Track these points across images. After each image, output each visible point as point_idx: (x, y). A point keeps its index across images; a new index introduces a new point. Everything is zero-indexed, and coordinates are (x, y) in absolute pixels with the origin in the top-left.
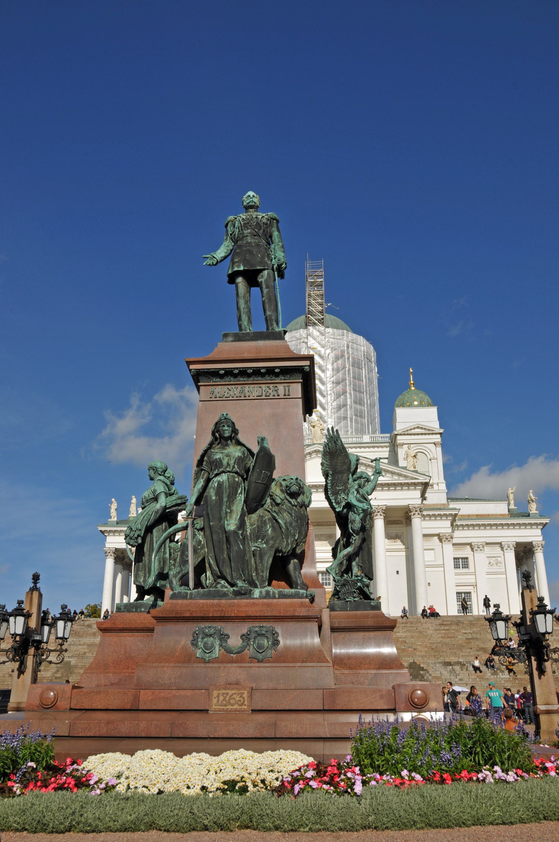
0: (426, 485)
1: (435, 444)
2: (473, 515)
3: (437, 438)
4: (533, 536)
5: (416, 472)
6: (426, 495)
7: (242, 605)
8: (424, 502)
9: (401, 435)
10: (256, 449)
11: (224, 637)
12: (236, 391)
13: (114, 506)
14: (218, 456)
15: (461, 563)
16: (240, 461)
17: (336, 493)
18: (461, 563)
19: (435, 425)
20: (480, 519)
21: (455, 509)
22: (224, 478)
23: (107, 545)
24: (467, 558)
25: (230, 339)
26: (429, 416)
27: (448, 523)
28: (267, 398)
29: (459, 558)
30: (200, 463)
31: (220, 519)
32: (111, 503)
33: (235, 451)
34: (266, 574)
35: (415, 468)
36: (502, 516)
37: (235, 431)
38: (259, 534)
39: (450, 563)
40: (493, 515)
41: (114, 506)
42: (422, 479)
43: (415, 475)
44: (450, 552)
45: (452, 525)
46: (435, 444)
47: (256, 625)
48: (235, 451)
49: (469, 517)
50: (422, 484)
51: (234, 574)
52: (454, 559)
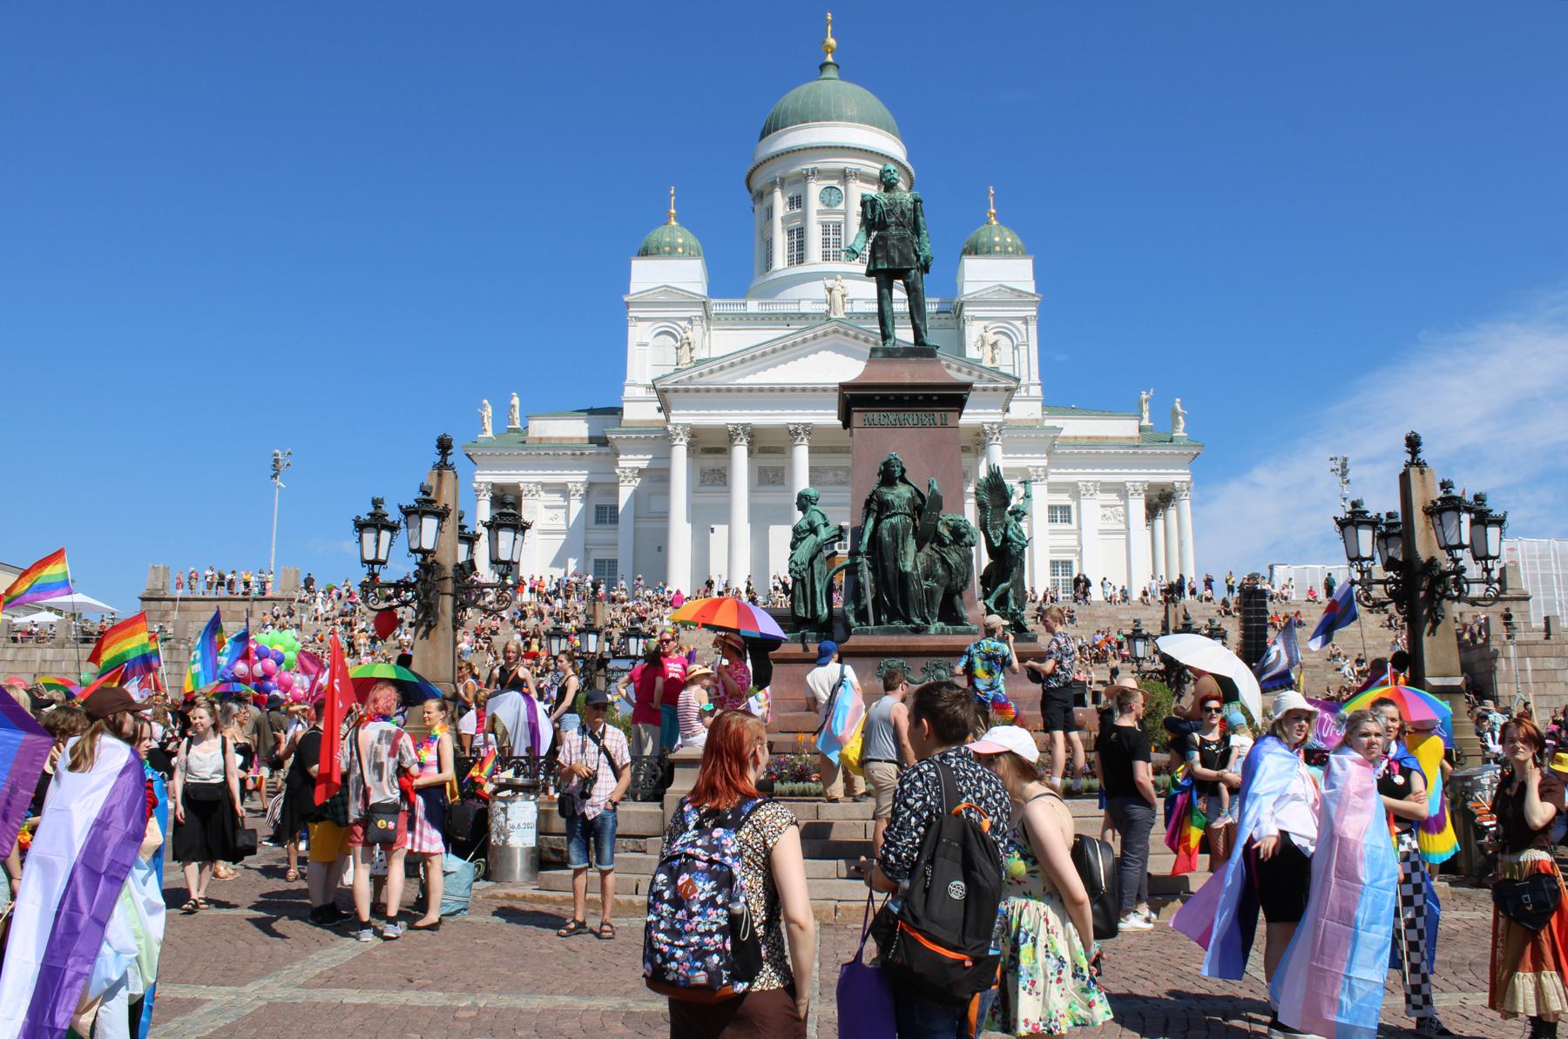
1: (1025, 320)
3: (1031, 312)
4: (1177, 477)
6: (1012, 405)
7: (921, 641)
8: (1007, 416)
9: (971, 303)
12: (892, 417)
13: (488, 412)
16: (911, 501)
17: (994, 528)
19: (1030, 287)
20: (1095, 442)
21: (1054, 428)
22: (894, 520)
23: (478, 479)
25: (880, 354)
26: (1019, 273)
28: (924, 426)
30: (868, 503)
31: (896, 560)
32: (483, 407)
34: (937, 611)
35: (993, 360)
37: (903, 471)
38: (928, 574)
41: (488, 412)
46: (1025, 320)
47: (935, 660)
49: (1075, 442)
50: (1007, 390)
51: (912, 612)
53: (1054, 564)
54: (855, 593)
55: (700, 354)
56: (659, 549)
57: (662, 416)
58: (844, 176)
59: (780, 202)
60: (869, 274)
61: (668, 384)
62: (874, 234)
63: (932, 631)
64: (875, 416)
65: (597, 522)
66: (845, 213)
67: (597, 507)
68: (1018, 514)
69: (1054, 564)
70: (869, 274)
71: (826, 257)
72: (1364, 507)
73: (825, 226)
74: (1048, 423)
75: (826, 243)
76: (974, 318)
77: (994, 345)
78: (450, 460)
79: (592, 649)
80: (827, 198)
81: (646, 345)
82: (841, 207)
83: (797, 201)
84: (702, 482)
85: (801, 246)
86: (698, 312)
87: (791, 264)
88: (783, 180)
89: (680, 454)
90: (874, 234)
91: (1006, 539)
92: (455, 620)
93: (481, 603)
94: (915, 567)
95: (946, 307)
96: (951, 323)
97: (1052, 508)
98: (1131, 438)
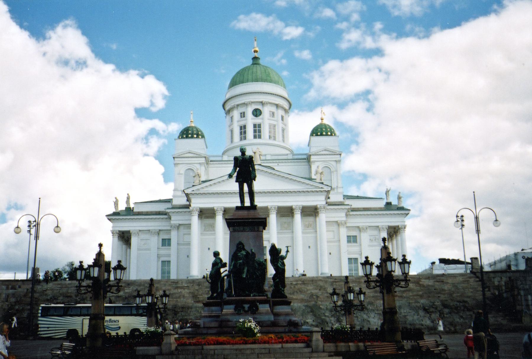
0: (328, 192)
2: (361, 208)
5: (322, 183)
8: (328, 200)
10: (250, 252)
11: (244, 308)
14: (239, 254)
15: (352, 239)
18: (352, 239)
21: (348, 205)
22: (241, 261)
24: (356, 236)
27: (343, 214)
29: (350, 236)
33: (244, 253)
35: (321, 180)
36: (380, 209)
37: (244, 246)
39: (344, 239)
40: (374, 208)
42: (326, 188)
43: (321, 186)
44: (344, 233)
45: (347, 215)
48: (244, 253)
52: (348, 236)
53: (350, 259)
54: (229, 283)
55: (203, 178)
56: (188, 256)
57: (188, 203)
58: (262, 103)
59: (236, 114)
60: (236, 181)
61: (188, 191)
62: (238, 169)
63: (252, 295)
64: (237, 228)
65: (162, 245)
66: (263, 119)
67: (163, 239)
68: (283, 258)
69: (350, 259)
70: (236, 181)
71: (255, 137)
72: (369, 259)
73: (255, 126)
74: (346, 203)
75: (255, 131)
76: (314, 162)
77: (321, 173)
78: (102, 250)
79: (150, 301)
80: (255, 113)
81: (182, 174)
82: (261, 117)
83: (243, 115)
84: (205, 230)
85: (245, 132)
86: (203, 160)
87: (241, 140)
88: (238, 105)
89: (195, 220)
90: (238, 169)
91: (278, 267)
92: (103, 295)
93: (111, 291)
94: (247, 276)
95: (305, 157)
96: (306, 164)
97: (348, 237)
98: (381, 208)
